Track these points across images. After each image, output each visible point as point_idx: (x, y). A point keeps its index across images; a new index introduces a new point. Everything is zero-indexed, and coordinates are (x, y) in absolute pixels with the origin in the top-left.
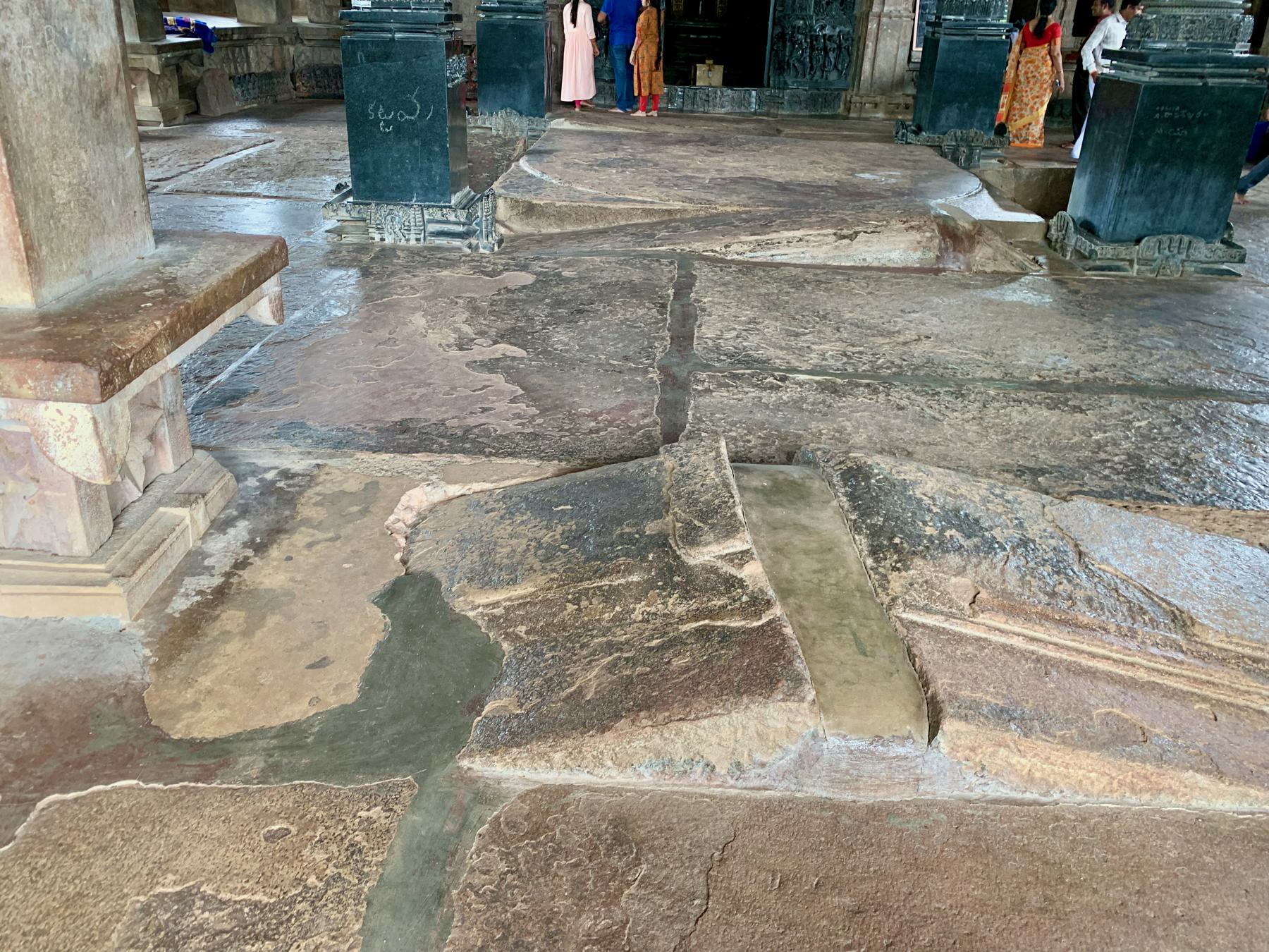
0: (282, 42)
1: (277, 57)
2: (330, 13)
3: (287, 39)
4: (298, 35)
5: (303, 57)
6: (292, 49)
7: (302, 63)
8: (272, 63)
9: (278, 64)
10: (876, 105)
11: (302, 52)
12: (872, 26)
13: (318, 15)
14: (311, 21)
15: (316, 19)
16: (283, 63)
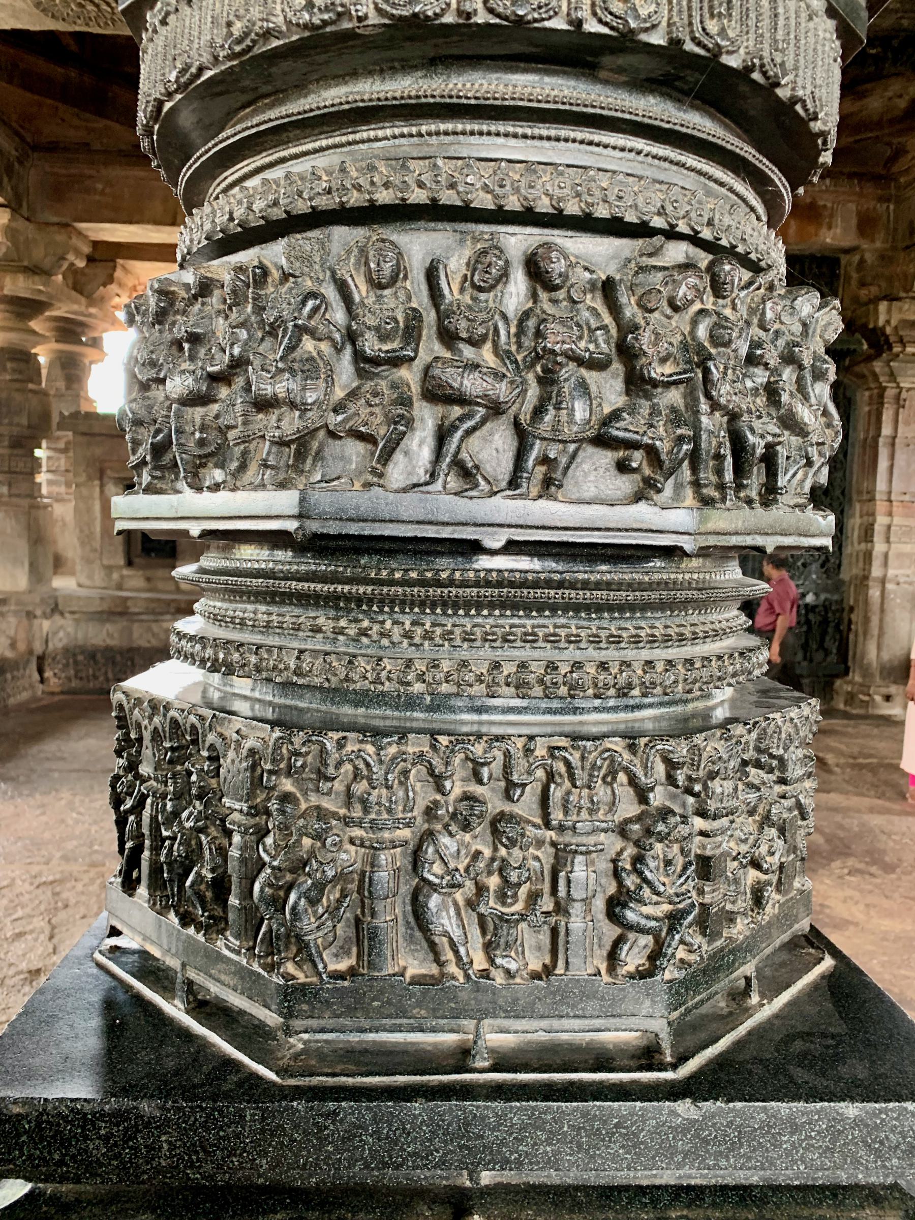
0: (30, 615)
1: (21, 636)
2: (109, 575)
3: (38, 612)
4: (55, 608)
5: (61, 634)
6: (46, 625)
7: (58, 643)
8: (13, 645)
9: (22, 646)
10: (888, 698)
11: (62, 627)
12: (874, 593)
13: (90, 577)
14: (80, 585)
15: (84, 580)
16: (30, 643)
